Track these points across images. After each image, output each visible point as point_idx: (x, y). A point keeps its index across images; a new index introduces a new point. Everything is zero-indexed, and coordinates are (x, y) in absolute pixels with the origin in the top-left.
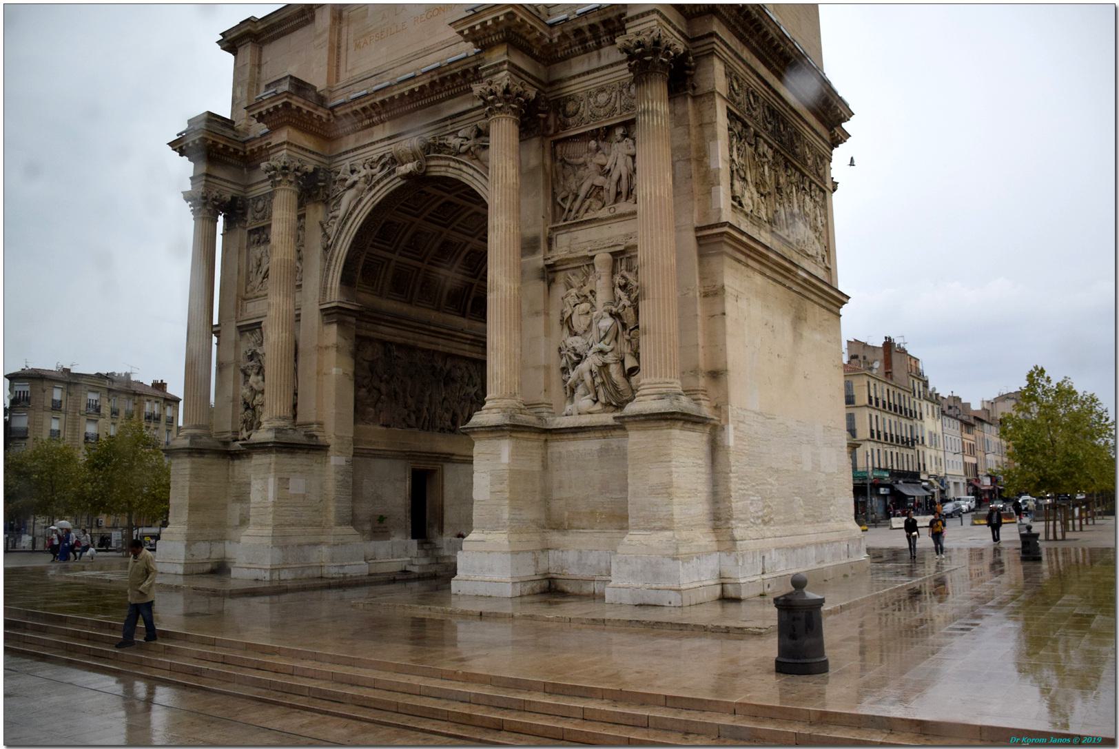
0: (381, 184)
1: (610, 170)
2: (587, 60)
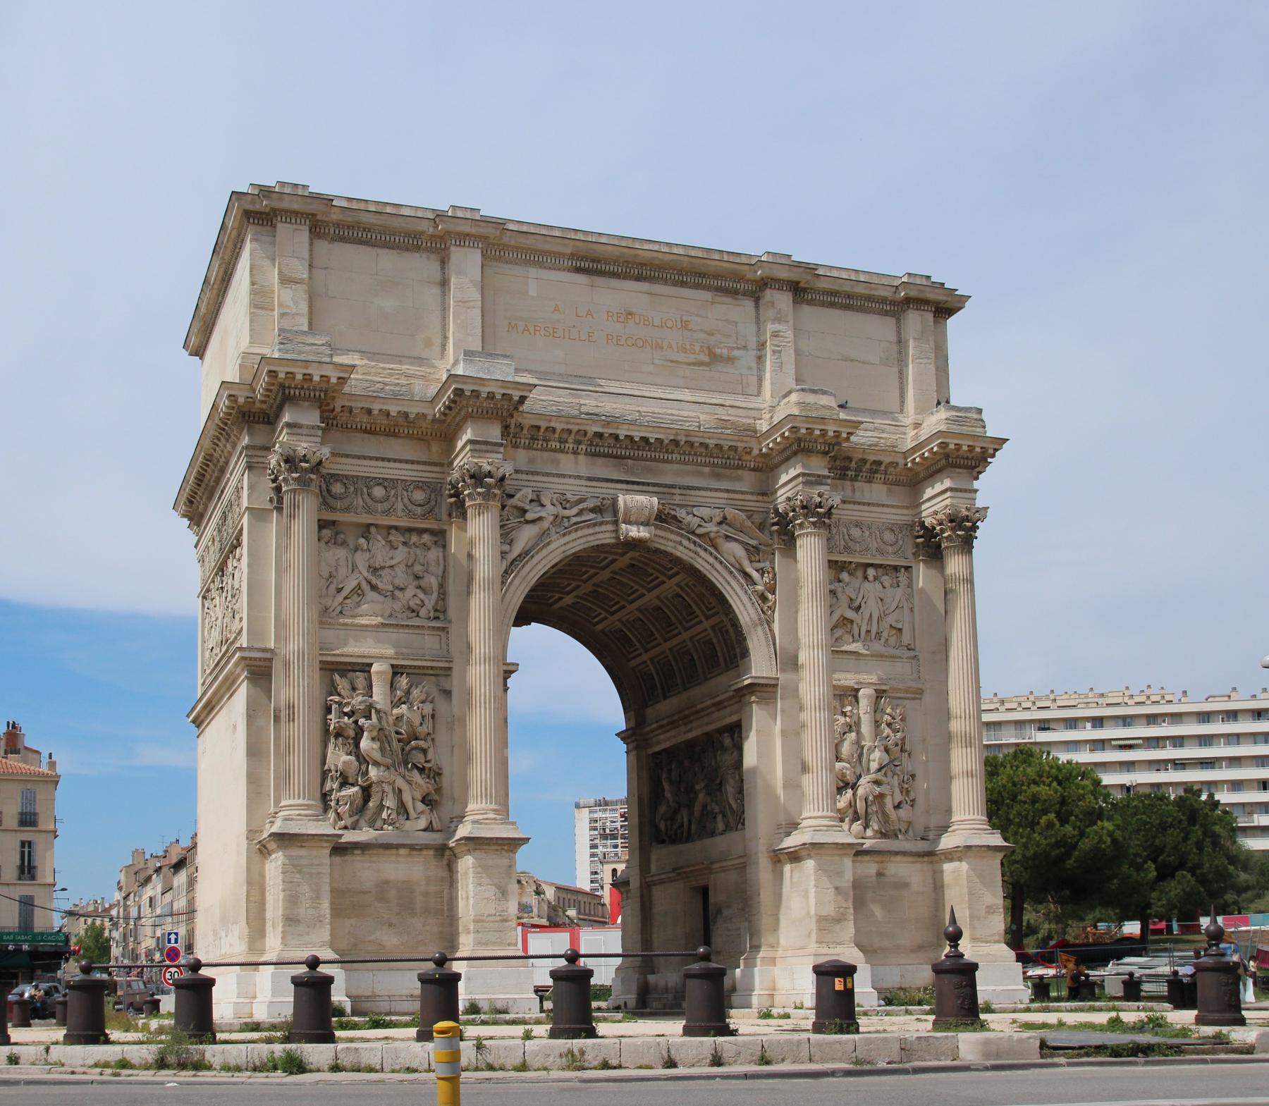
0: (580, 533)
1: (860, 607)
2: (840, 487)
